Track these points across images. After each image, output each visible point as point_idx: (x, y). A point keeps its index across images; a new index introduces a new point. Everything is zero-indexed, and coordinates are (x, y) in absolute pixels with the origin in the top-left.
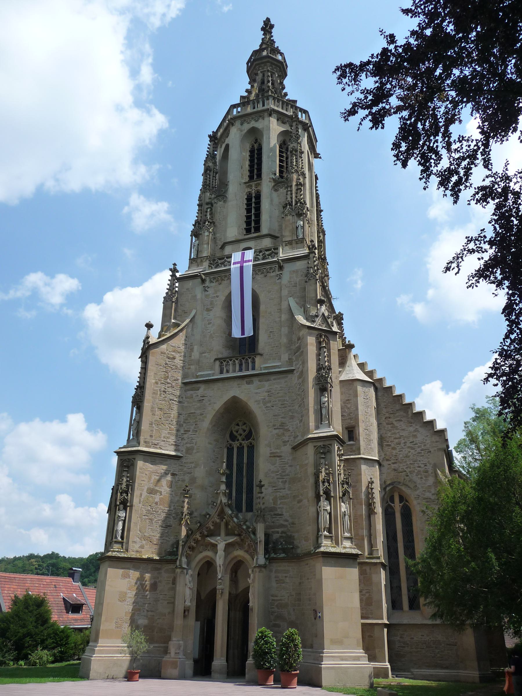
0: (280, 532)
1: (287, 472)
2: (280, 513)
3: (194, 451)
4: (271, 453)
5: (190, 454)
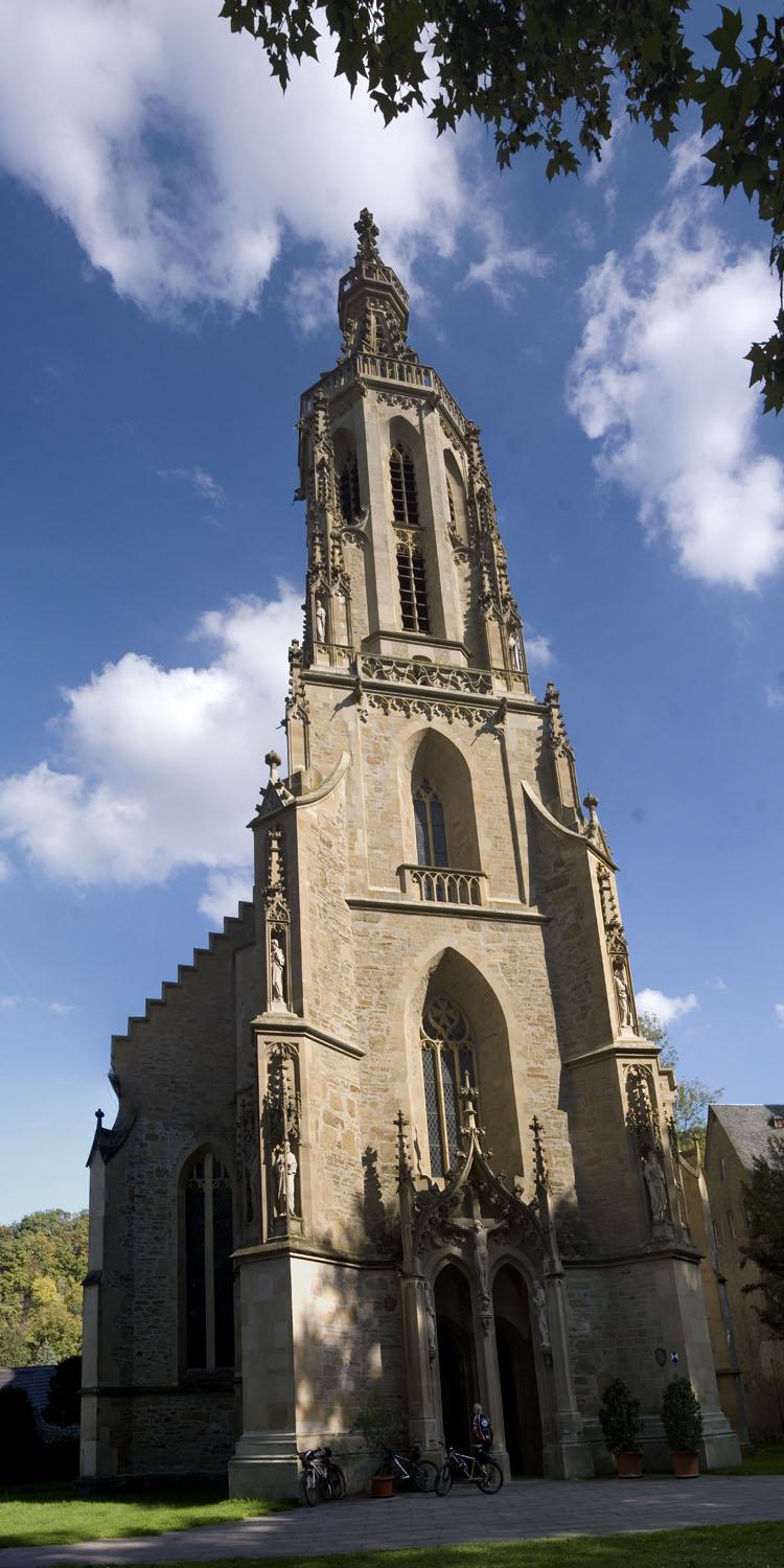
3: (387, 1047)
4: (530, 1069)
5: (382, 1052)
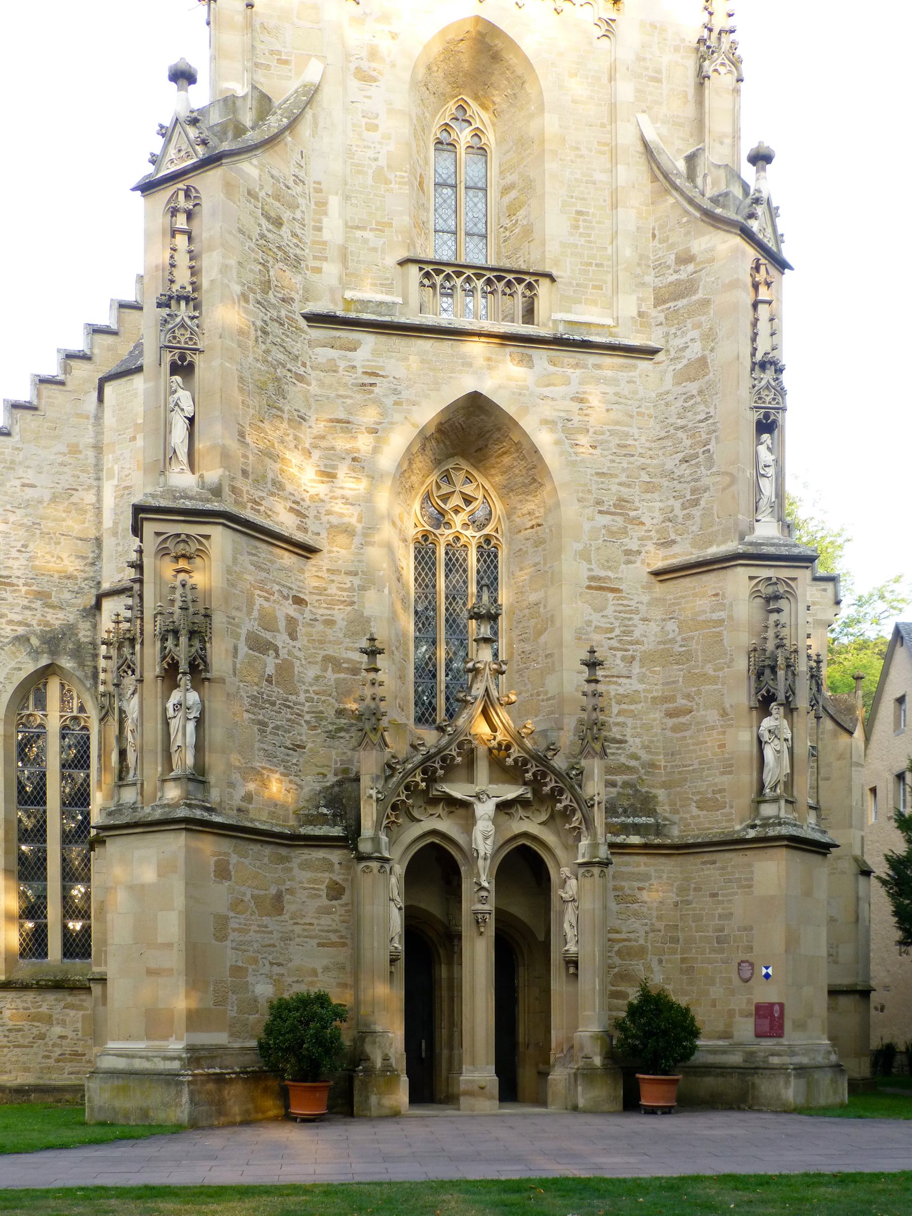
0: (620, 783)
1: (637, 634)
2: (618, 737)
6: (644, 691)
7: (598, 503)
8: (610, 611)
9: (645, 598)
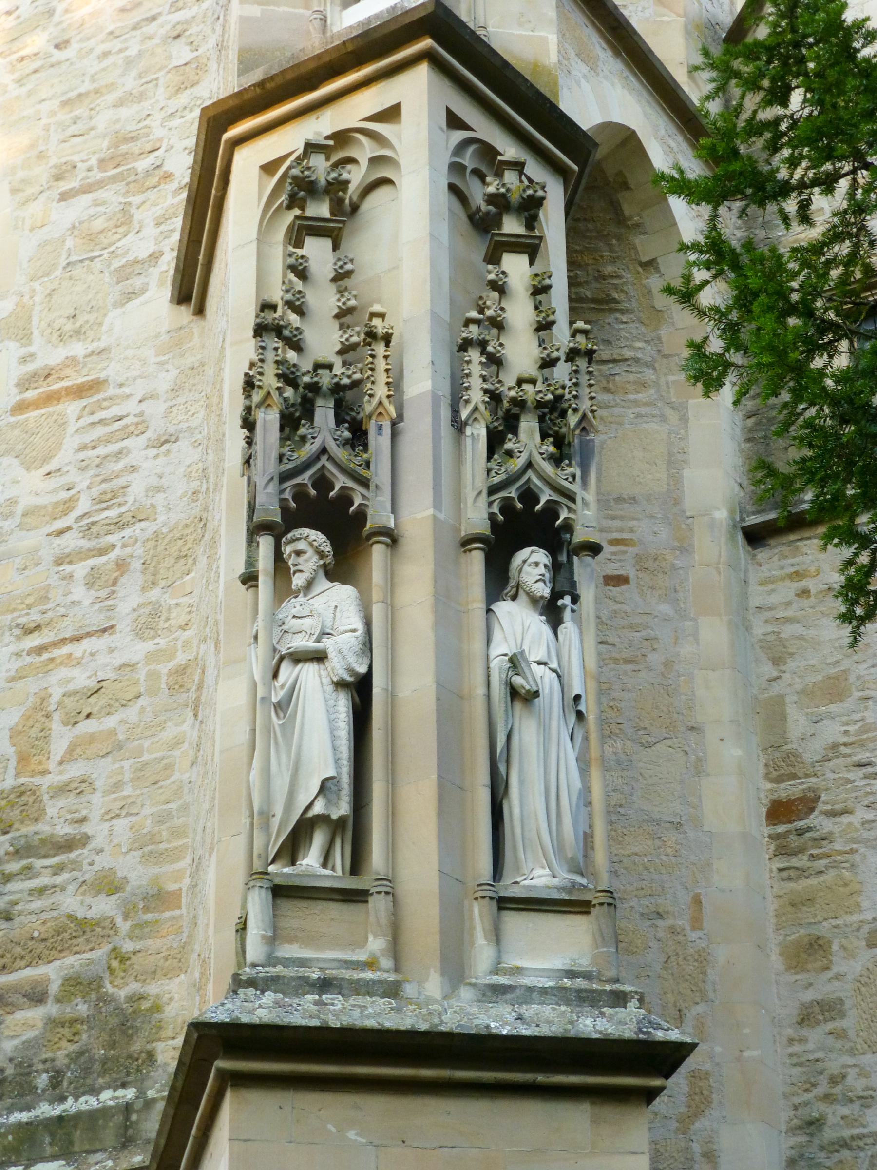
0: (54, 988)
2: (63, 830)
6: (152, 657)
7: (58, 178)
8: (66, 455)
9: (164, 381)
